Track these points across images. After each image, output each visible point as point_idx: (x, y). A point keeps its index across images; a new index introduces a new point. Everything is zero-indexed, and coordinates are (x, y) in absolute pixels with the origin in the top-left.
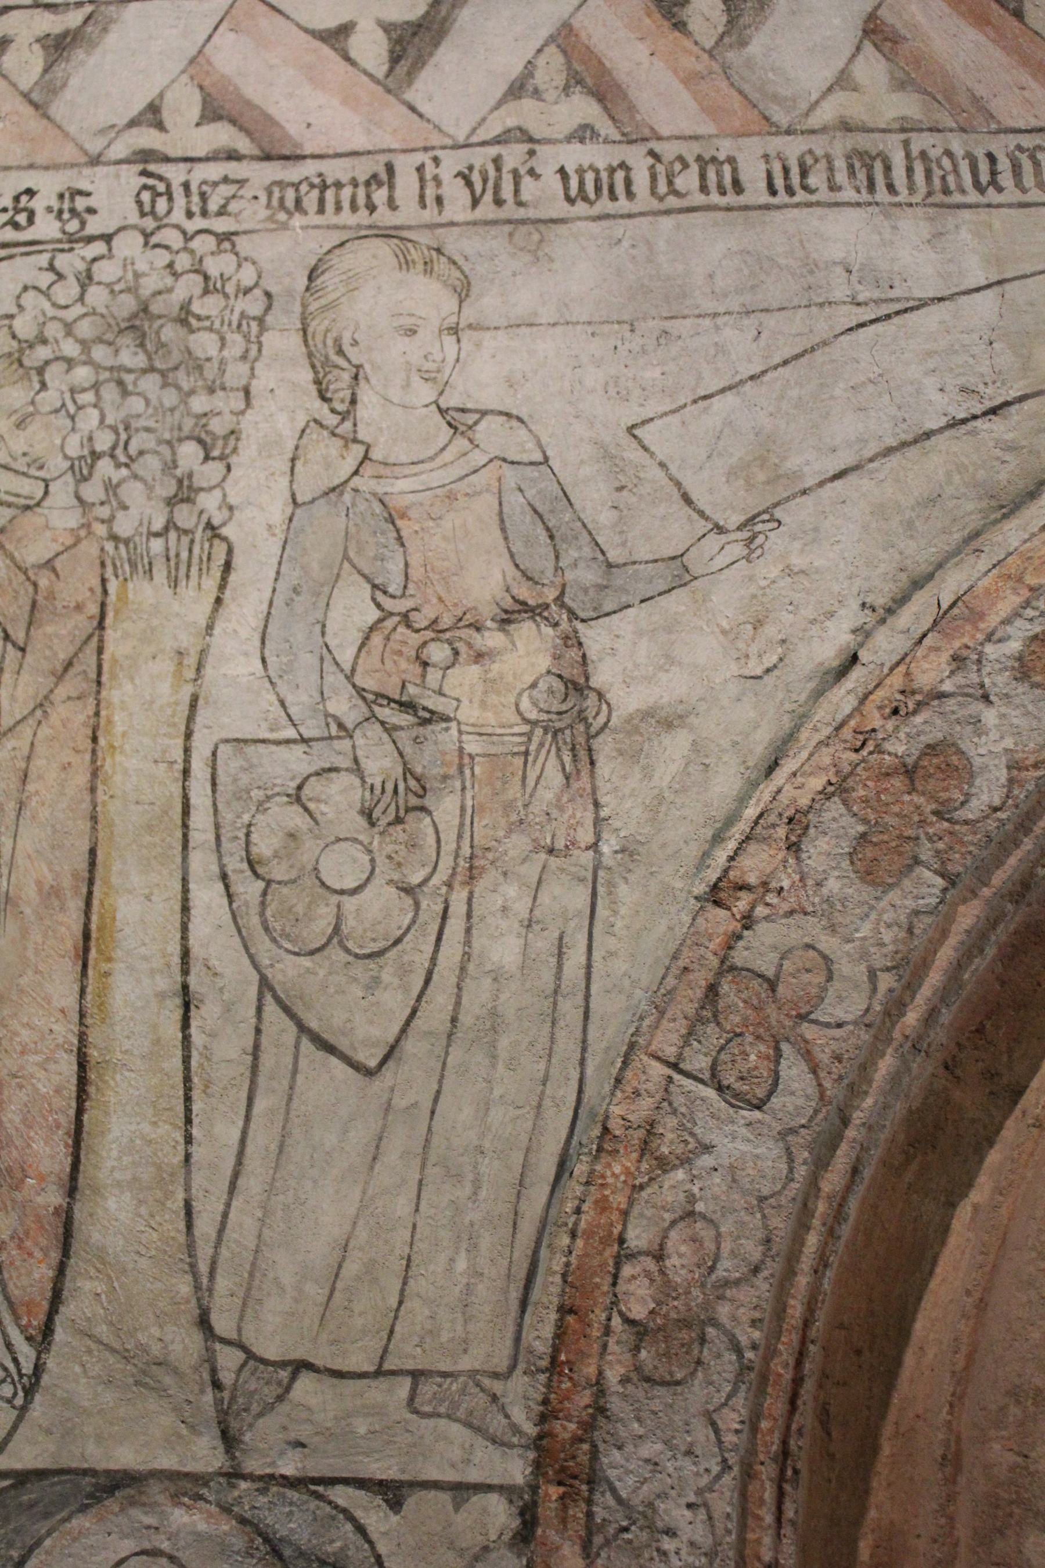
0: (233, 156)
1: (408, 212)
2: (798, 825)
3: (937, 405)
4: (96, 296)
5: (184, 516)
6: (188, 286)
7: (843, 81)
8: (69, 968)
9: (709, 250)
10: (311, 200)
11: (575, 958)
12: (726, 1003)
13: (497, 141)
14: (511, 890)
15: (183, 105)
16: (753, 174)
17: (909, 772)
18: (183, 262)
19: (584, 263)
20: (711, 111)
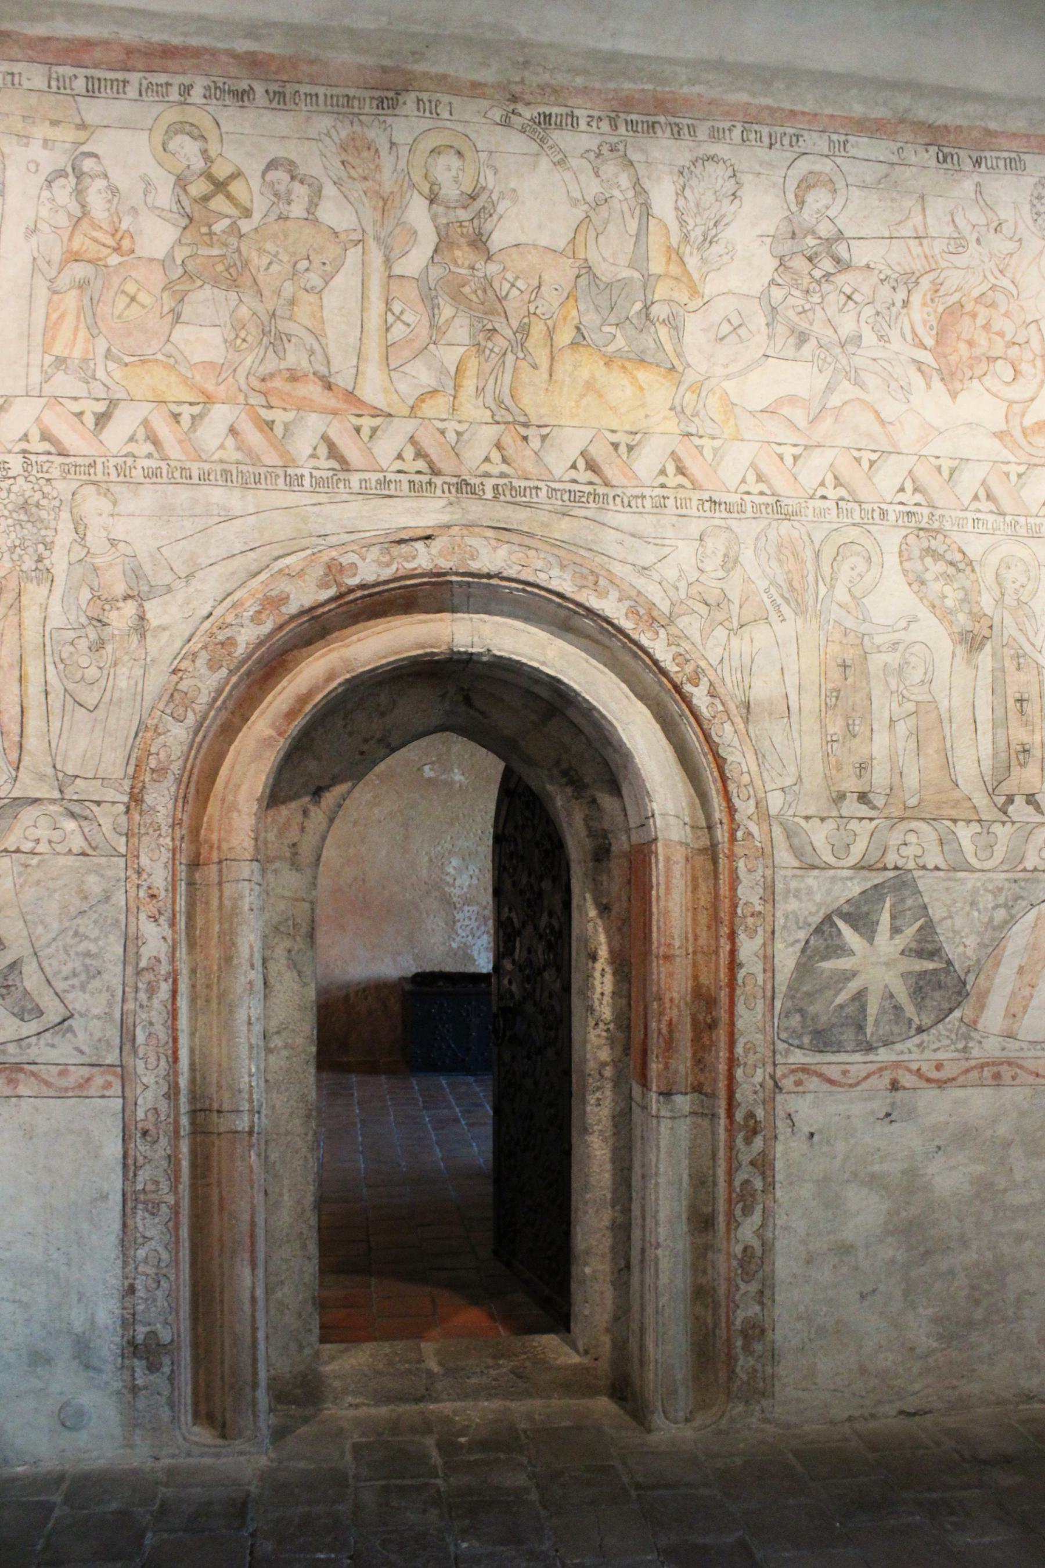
0: (49, 453)
1: (100, 477)
2: (195, 655)
3: (238, 547)
4: (12, 496)
5: (40, 566)
6: (38, 496)
7: (222, 447)
8: (17, 684)
9: (183, 496)
10: (72, 470)
11: (140, 686)
12: (175, 698)
13: (125, 456)
14: (125, 669)
15: (35, 435)
16: (195, 474)
17: (222, 644)
18: (37, 487)
19: (148, 497)
20: (186, 453)
